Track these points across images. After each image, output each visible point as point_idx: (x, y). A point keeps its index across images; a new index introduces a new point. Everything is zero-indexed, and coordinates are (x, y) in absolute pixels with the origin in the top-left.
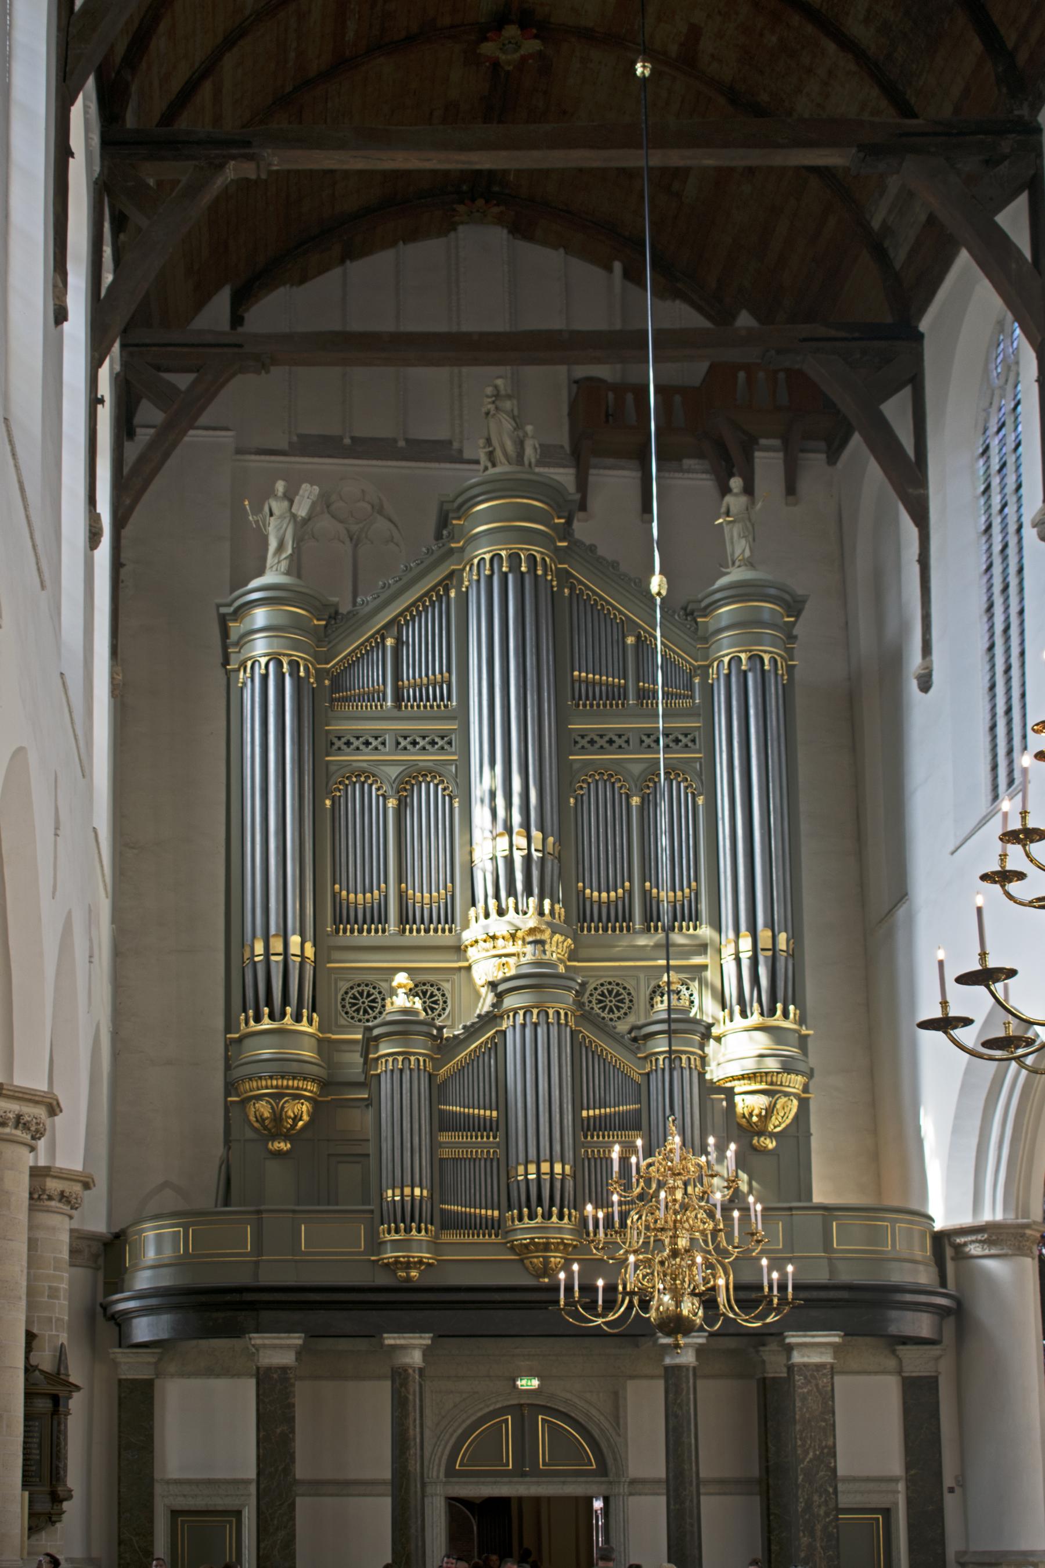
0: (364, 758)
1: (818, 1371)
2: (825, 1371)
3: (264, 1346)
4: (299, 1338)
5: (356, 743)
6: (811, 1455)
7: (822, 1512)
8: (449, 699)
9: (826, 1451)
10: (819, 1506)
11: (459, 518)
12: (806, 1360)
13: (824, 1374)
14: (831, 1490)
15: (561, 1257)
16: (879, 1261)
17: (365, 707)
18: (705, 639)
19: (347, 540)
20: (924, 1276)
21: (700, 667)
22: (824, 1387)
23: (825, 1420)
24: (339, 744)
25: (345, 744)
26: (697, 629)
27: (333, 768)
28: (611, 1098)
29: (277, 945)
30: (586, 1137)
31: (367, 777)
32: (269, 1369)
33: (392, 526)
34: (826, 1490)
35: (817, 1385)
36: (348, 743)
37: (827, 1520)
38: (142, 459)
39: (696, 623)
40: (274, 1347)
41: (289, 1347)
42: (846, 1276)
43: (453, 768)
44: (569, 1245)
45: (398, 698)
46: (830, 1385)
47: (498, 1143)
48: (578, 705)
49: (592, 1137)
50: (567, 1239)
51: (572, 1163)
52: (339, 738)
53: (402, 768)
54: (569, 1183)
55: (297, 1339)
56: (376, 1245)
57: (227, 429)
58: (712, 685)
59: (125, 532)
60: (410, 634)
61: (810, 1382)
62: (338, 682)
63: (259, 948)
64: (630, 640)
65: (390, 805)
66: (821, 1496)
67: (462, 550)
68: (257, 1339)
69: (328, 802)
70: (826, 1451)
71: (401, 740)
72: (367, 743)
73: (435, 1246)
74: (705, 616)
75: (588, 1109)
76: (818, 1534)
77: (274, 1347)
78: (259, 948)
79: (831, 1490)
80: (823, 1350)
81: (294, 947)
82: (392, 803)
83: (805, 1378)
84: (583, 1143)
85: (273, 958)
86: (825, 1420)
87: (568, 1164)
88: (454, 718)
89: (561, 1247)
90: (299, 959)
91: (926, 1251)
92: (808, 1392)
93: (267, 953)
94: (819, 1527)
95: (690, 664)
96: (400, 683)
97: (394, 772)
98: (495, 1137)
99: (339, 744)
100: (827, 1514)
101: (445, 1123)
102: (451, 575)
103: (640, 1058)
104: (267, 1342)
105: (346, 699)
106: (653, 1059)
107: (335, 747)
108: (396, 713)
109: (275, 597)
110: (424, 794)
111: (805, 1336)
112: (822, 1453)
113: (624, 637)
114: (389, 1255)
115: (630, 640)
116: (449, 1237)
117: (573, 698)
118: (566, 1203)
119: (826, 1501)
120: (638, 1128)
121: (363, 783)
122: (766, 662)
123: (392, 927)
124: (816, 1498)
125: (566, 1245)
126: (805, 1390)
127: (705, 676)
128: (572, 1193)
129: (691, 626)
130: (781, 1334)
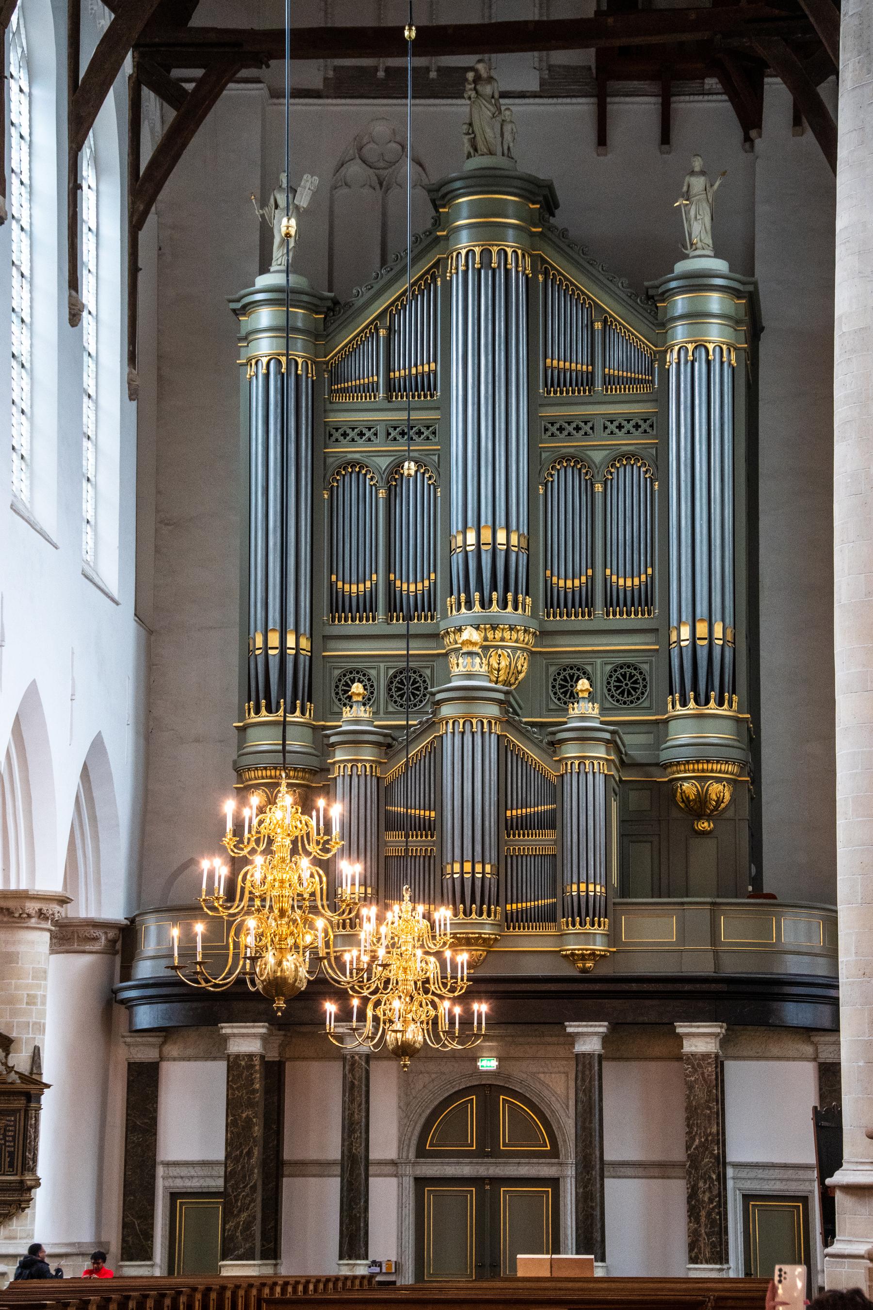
1: (703, 1060)
2: (710, 1061)
3: (234, 1035)
4: (263, 1027)
5: (352, 434)
6: (697, 1142)
7: (706, 1199)
8: (435, 389)
9: (710, 1138)
10: (704, 1192)
11: (444, 207)
12: (693, 1049)
13: (709, 1063)
14: (714, 1177)
15: (483, 951)
17: (360, 400)
18: (663, 325)
19: (378, 187)
21: (655, 353)
22: (708, 1075)
23: (710, 1108)
24: (337, 435)
25: (342, 435)
26: (656, 313)
27: (330, 460)
28: (532, 799)
29: (274, 639)
30: (509, 836)
31: (361, 468)
32: (237, 1056)
33: (420, 169)
34: (710, 1178)
35: (703, 1074)
36: (345, 435)
37: (711, 1206)
38: (154, 163)
39: (657, 307)
40: (243, 1035)
41: (254, 1035)
42: (732, 968)
43: (436, 458)
44: (489, 939)
46: (714, 1073)
47: (434, 842)
48: (549, 392)
49: (514, 836)
50: (485, 934)
51: (494, 861)
52: (337, 429)
53: (392, 458)
55: (261, 1029)
57: (260, 82)
58: (668, 370)
59: (141, 234)
61: (697, 1071)
62: (336, 374)
63: (259, 642)
64: (598, 325)
65: (380, 496)
66: (705, 1183)
67: (447, 238)
68: (227, 1029)
70: (710, 1138)
71: (391, 430)
72: (361, 434)
74: (663, 301)
75: (512, 809)
76: (703, 1219)
77: (243, 1035)
78: (259, 642)
79: (714, 1177)
80: (708, 1040)
82: (382, 494)
83: (693, 1067)
84: (506, 841)
85: (271, 652)
86: (710, 1108)
87: (490, 863)
88: (438, 408)
89: (480, 941)
90: (294, 652)
92: (695, 1081)
93: (266, 648)
94: (703, 1213)
95: (650, 348)
96: (392, 374)
97: (384, 463)
98: (432, 837)
99: (337, 435)
100: (711, 1201)
101: (391, 823)
102: (436, 265)
103: (556, 761)
104: (236, 1031)
105: (344, 390)
106: (569, 763)
107: (333, 439)
108: (386, 405)
111: (691, 1027)
112: (707, 1140)
113: (592, 323)
115: (598, 325)
117: (546, 386)
118: (486, 900)
119: (710, 1188)
120: (553, 827)
121: (359, 472)
122: (711, 353)
124: (701, 1184)
125: (484, 939)
126: (693, 1079)
127: (663, 361)
128: (494, 890)
129: (651, 311)
130: (672, 1024)
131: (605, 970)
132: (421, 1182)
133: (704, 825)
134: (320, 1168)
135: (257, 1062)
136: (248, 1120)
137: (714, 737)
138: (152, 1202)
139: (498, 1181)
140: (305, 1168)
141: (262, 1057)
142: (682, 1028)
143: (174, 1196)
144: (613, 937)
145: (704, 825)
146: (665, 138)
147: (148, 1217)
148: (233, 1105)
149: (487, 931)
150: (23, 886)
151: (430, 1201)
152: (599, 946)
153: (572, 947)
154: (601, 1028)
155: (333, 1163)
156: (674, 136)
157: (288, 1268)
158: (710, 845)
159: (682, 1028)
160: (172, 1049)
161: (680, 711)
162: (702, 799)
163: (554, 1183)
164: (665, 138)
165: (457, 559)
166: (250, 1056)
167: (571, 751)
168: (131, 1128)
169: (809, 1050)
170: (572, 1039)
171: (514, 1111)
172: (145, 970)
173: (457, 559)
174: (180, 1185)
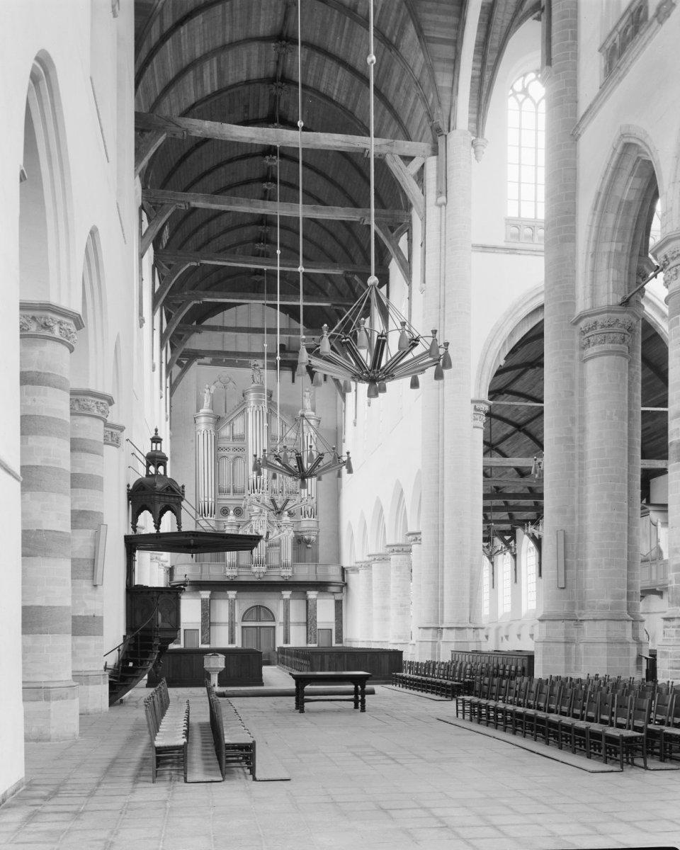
0: (226, 452)
16: (328, 575)
20: (339, 579)
29: (206, 499)
45: (233, 438)
54: (265, 559)
55: (209, 592)
56: (225, 572)
68: (202, 592)
73: (238, 572)
81: (210, 499)
91: (339, 572)
97: (232, 457)
109: (207, 415)
110: (239, 461)
114: (228, 574)
123: (232, 493)
131: (291, 580)
132: (243, 627)
133: (309, 546)
134: (220, 624)
137: (312, 525)
139: (260, 627)
140: (298, 624)
142: (309, 593)
143: (185, 630)
144: (293, 572)
145: (309, 546)
146: (293, 381)
152: (290, 574)
153: (283, 574)
154: (290, 592)
155: (226, 623)
156: (295, 381)
158: (310, 550)
159: (309, 593)
161: (304, 519)
162: (309, 540)
163: (274, 627)
164: (293, 381)
165: (251, 482)
166: (207, 599)
167: (283, 528)
169: (333, 597)
170: (282, 595)
171: (265, 612)
173: (251, 482)
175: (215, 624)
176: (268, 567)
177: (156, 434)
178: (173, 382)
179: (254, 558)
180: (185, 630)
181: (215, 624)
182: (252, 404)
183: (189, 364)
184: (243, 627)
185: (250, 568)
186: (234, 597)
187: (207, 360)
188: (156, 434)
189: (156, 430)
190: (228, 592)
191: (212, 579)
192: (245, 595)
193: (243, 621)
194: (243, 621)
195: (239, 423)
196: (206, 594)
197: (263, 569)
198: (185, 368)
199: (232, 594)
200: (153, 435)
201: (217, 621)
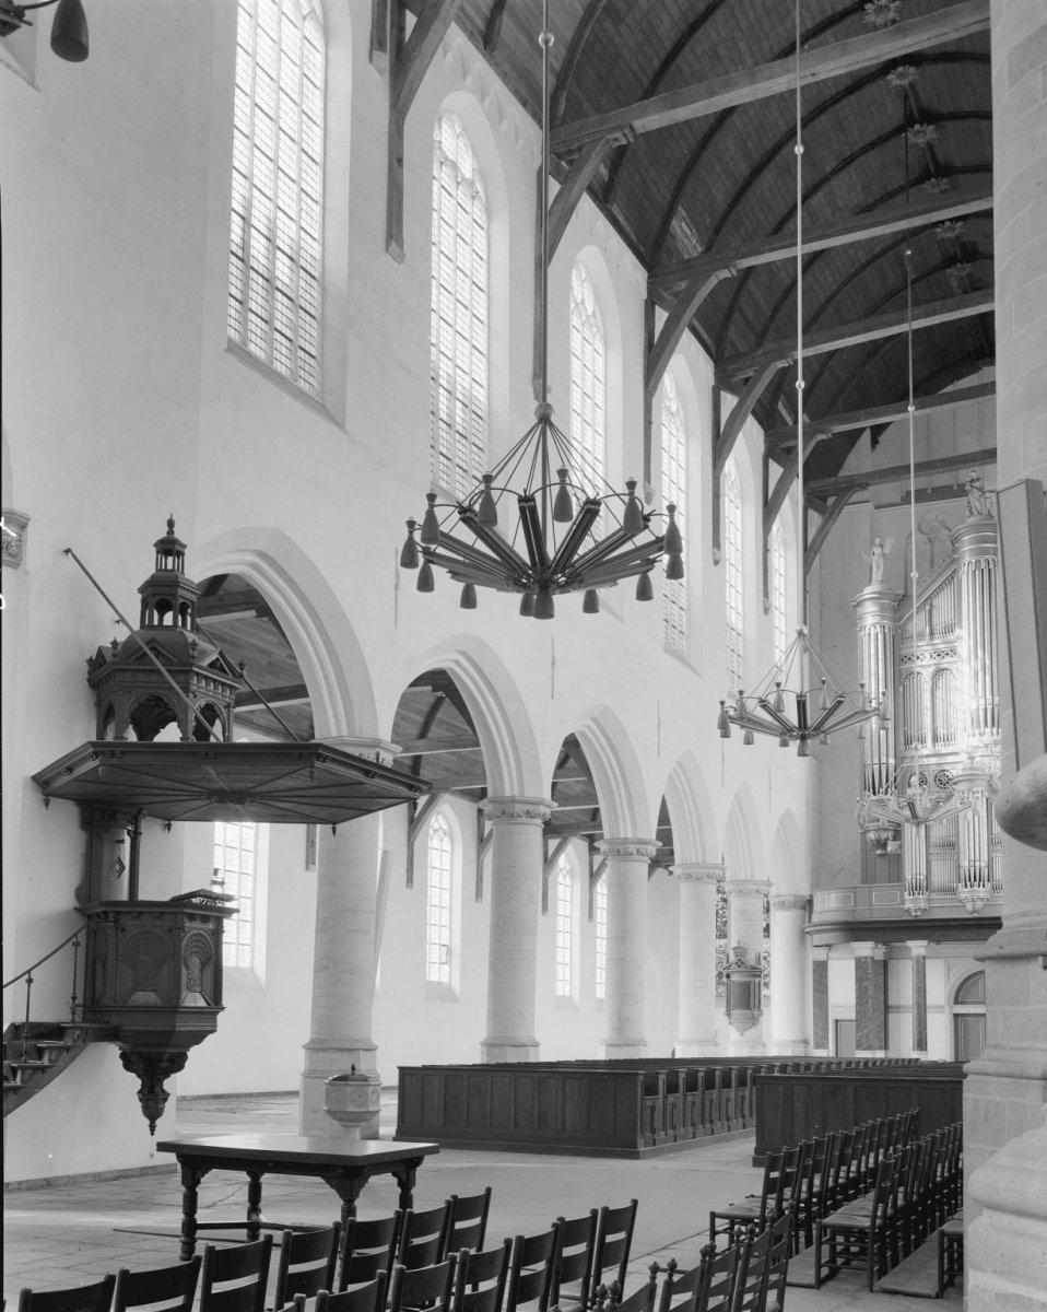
55: (870, 944)
56: (903, 902)
60: (935, 602)
69: (901, 689)
114: (908, 905)
116: (934, 896)
135: (869, 960)
136: (866, 987)
138: (827, 1024)
141: (872, 958)
143: (837, 1021)
147: (826, 1029)
148: (859, 980)
149: (982, 895)
150: (749, 878)
151: (961, 1024)
157: (893, 1055)
160: (832, 954)
168: (815, 991)
172: (816, 918)
174: (839, 1018)
175: (898, 1009)
176: (995, 889)
177: (171, 532)
178: (810, 540)
179: (962, 872)
180: (837, 1021)
181: (898, 1009)
182: (967, 559)
183: (838, 507)
184: (955, 1015)
185: (953, 891)
186: (922, 952)
187: (888, 490)
188: (171, 532)
189: (171, 524)
190: (910, 943)
191: (876, 917)
192: (948, 948)
193: (957, 1002)
194: (957, 1002)
195: (943, 602)
196: (865, 949)
197: (982, 892)
198: (830, 516)
199: (917, 947)
200: (162, 533)
201: (902, 1003)
